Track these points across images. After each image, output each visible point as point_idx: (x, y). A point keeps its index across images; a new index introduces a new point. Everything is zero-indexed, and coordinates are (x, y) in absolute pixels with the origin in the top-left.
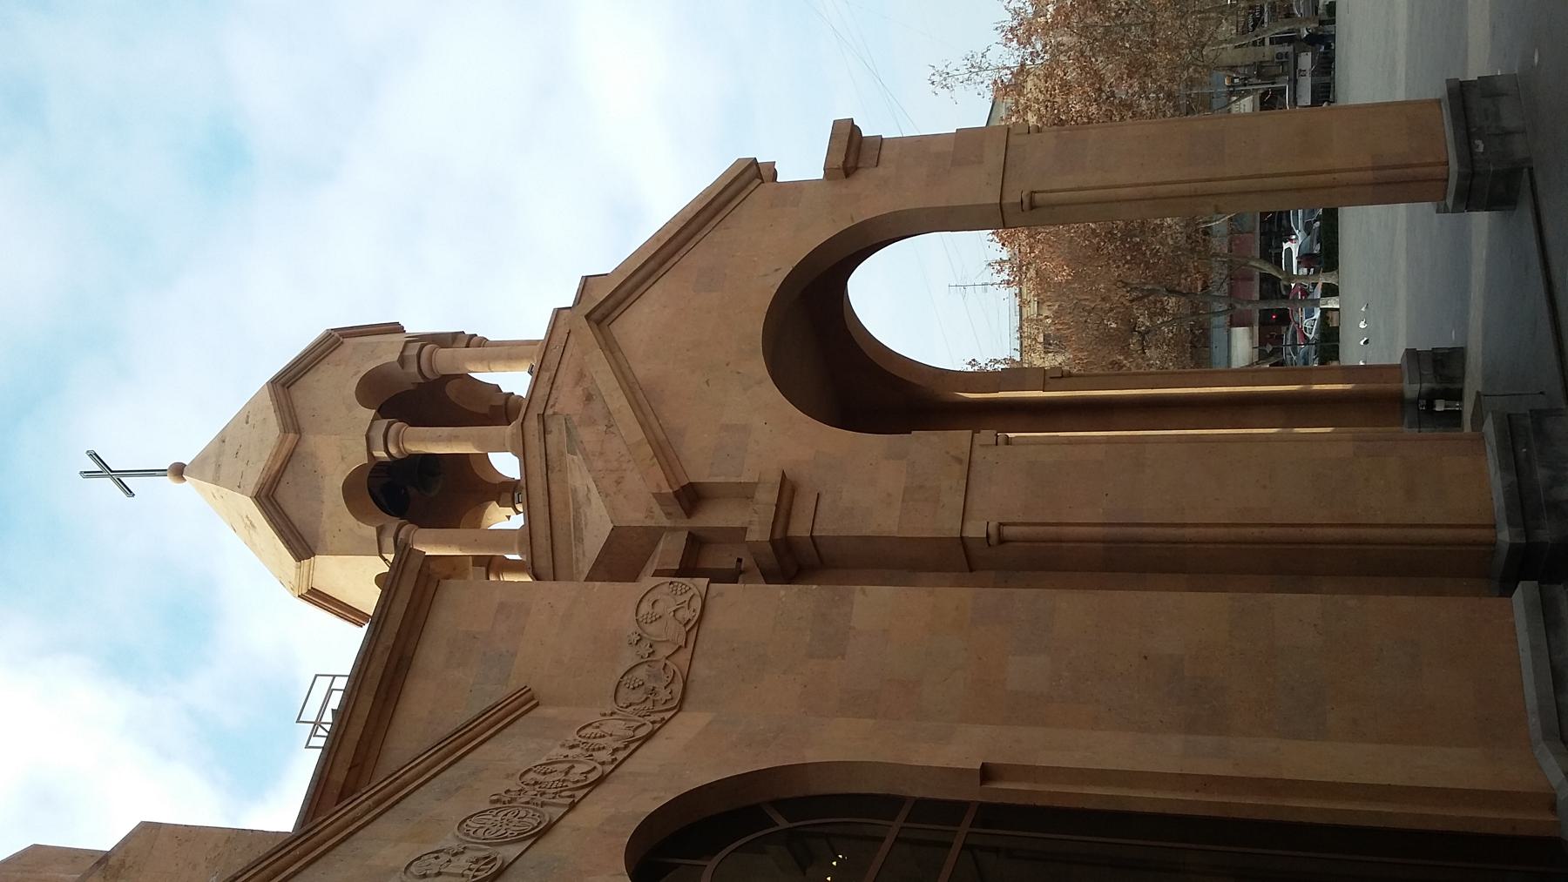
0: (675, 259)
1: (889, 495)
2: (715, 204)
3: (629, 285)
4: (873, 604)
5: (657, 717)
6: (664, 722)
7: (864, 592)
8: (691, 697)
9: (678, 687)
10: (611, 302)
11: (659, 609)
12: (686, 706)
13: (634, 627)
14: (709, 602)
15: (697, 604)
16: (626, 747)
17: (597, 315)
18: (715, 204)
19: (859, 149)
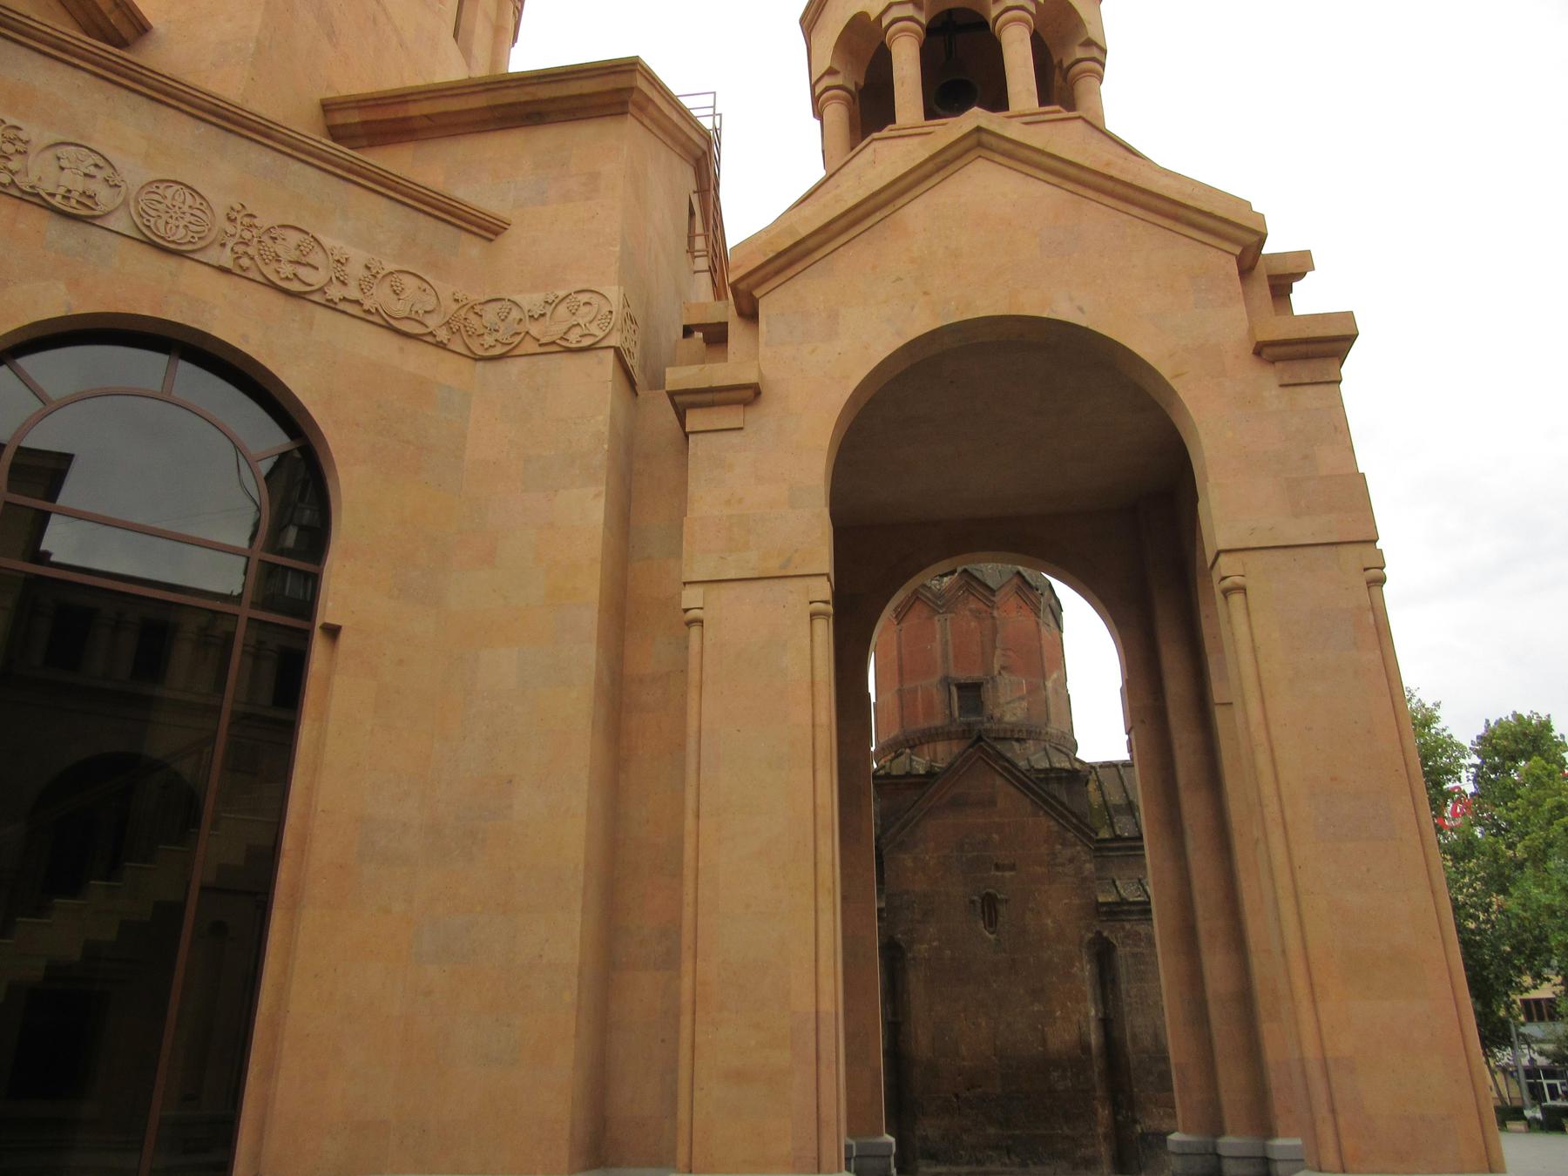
0: (1090, 193)
1: (740, 501)
2: (1181, 211)
3: (1037, 158)
4: (587, 509)
5: (443, 335)
6: (441, 345)
7: (597, 495)
8: (489, 365)
9: (498, 350)
10: (1007, 146)
11: (587, 308)
12: (480, 364)
13: (562, 294)
14: (592, 354)
15: (587, 342)
16: (369, 312)
17: (985, 138)
18: (1181, 211)
19: (1325, 356)
